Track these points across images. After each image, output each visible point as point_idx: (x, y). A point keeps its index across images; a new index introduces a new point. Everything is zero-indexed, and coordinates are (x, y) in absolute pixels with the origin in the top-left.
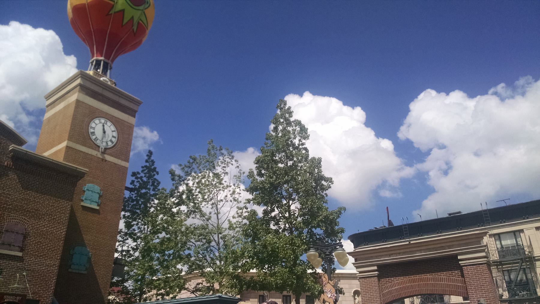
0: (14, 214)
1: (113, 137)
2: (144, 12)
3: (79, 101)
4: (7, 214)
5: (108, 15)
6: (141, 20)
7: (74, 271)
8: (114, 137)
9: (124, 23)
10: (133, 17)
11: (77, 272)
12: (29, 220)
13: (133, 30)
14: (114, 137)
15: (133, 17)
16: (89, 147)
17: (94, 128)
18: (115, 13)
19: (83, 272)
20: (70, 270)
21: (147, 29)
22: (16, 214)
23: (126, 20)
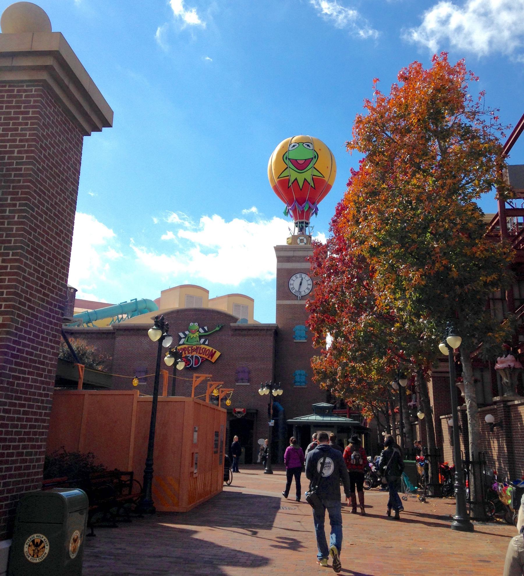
1: (308, 285)
2: (314, 168)
5: (289, 188)
6: (313, 175)
7: (298, 387)
8: (310, 285)
9: (301, 188)
10: (305, 179)
11: (300, 387)
13: (311, 186)
14: (310, 285)
15: (305, 179)
16: (292, 299)
17: (293, 284)
18: (292, 183)
19: (303, 387)
20: (295, 387)
21: (324, 177)
23: (301, 184)
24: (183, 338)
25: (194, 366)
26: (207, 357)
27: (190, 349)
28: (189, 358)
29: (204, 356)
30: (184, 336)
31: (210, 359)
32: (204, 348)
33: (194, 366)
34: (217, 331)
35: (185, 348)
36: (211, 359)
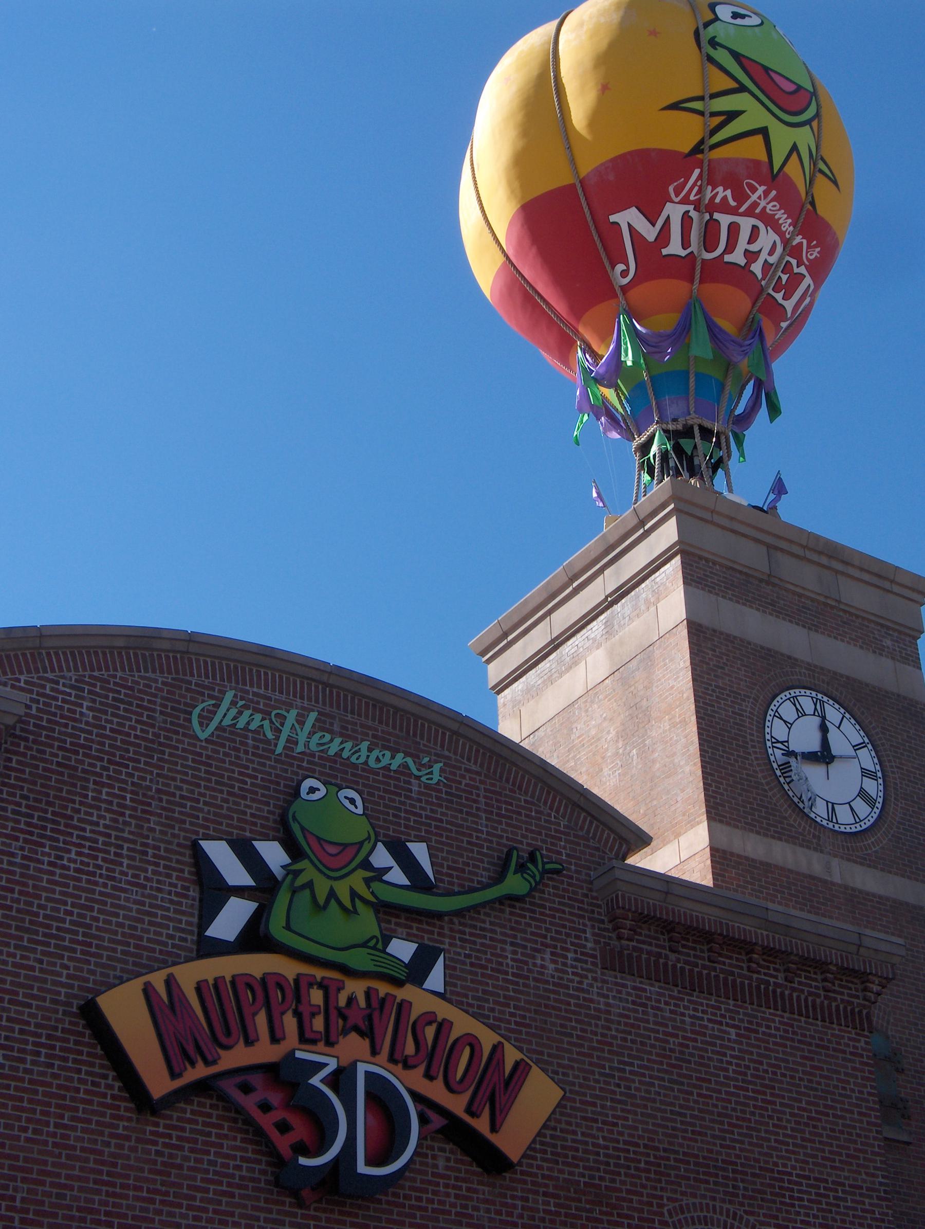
0: (694, 1195)
1: (865, 773)
3: (700, 625)
4: (669, 1199)
12: (752, 1219)
22: (703, 1196)
24: (240, 891)
25: (362, 1168)
26: (457, 1104)
27: (317, 997)
28: (316, 1081)
29: (436, 1091)
30: (247, 880)
31: (482, 1125)
32: (429, 1018)
33: (362, 1168)
34: (512, 899)
35: (279, 981)
36: (494, 1128)
